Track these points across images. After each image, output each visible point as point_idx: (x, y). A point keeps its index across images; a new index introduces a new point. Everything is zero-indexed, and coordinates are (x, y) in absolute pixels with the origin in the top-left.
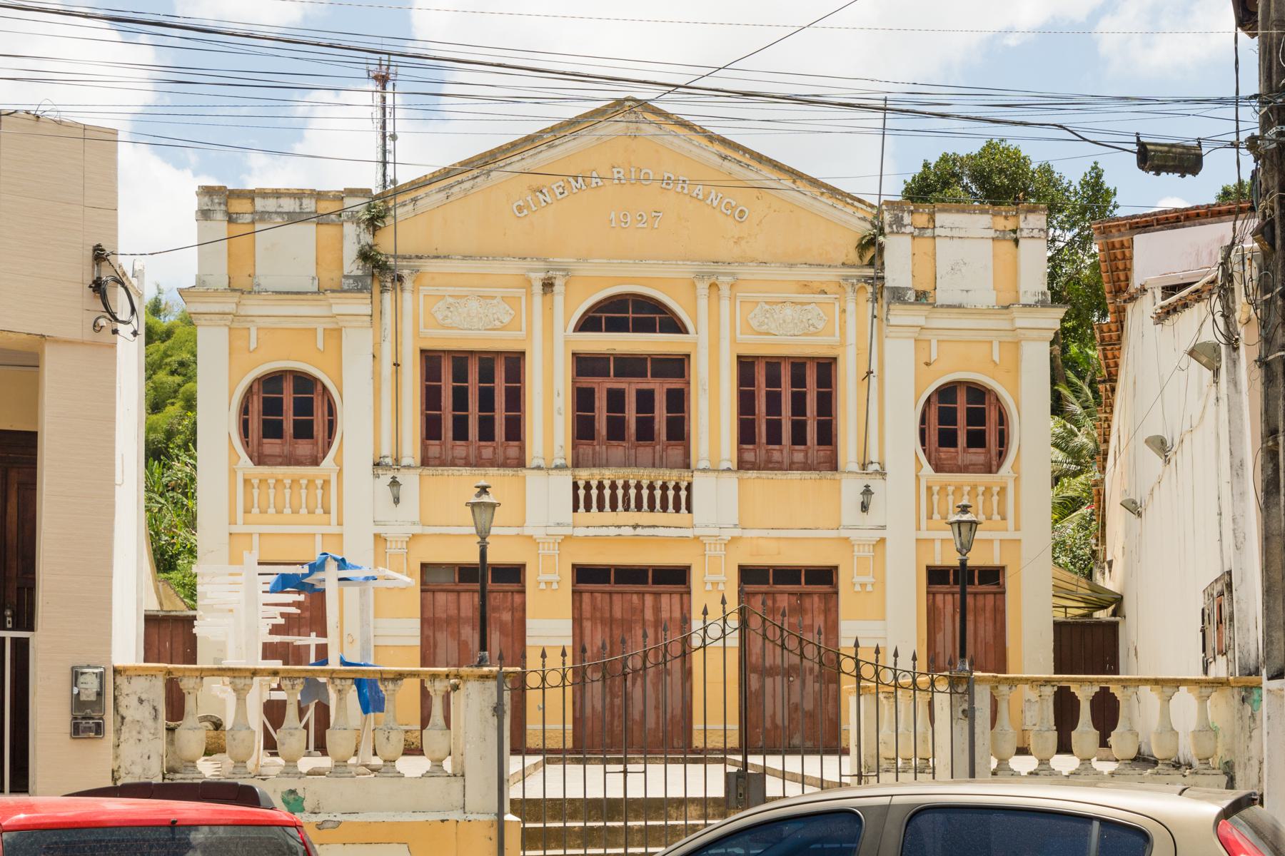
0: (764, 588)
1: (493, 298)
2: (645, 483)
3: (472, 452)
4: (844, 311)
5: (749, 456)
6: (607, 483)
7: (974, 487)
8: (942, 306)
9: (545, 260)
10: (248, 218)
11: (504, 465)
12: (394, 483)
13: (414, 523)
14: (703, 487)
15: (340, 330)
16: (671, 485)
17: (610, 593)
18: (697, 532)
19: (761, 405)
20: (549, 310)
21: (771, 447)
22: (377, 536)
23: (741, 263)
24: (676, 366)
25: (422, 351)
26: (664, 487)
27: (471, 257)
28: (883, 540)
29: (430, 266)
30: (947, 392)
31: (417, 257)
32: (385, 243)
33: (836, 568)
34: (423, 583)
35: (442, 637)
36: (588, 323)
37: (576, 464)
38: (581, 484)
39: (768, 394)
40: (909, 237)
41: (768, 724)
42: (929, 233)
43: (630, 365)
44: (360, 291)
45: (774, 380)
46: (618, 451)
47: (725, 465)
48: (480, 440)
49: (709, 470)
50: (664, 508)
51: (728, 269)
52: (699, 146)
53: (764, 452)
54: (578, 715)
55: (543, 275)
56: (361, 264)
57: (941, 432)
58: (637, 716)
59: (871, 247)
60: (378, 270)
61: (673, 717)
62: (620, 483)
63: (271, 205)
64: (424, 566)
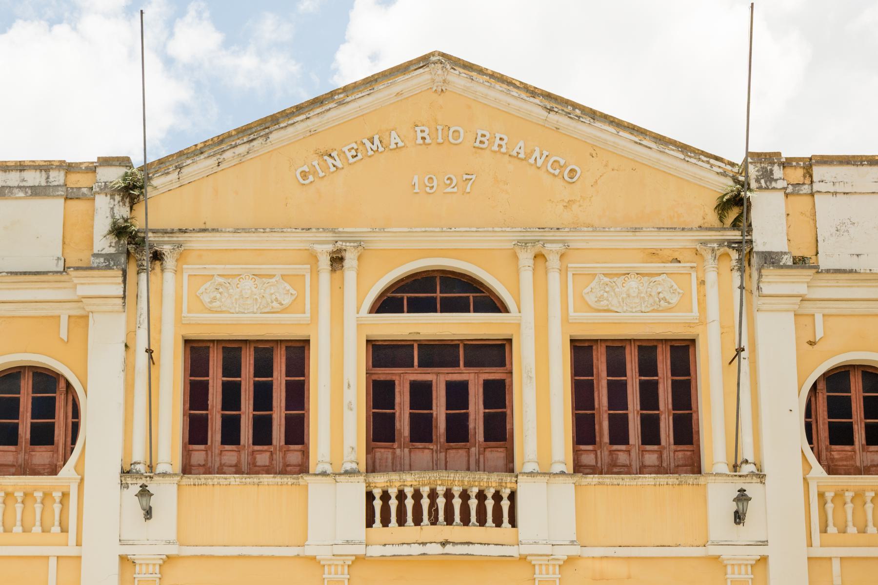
1: (272, 276)
2: (457, 490)
3: (245, 457)
4: (703, 282)
5: (588, 459)
6: (409, 491)
9: (333, 231)
11: (283, 472)
12: (144, 492)
14: (531, 496)
15: (86, 317)
16: (490, 493)
18: (524, 550)
19: (602, 397)
20: (338, 290)
21: (615, 447)
22: (123, 559)
23: (575, 229)
24: (496, 352)
25: (187, 342)
26: (481, 496)
27: (246, 230)
28: (764, 559)
29: (197, 242)
36: (387, 303)
37: (372, 468)
38: (377, 493)
39: (610, 384)
40: (781, 194)
42: (806, 189)
43: (438, 353)
45: (616, 367)
46: (423, 454)
47: (557, 468)
48: (254, 444)
49: (538, 474)
51: (558, 236)
53: (606, 453)
55: (330, 247)
56: (113, 239)
57: (832, 427)
59: (735, 205)
60: (135, 247)
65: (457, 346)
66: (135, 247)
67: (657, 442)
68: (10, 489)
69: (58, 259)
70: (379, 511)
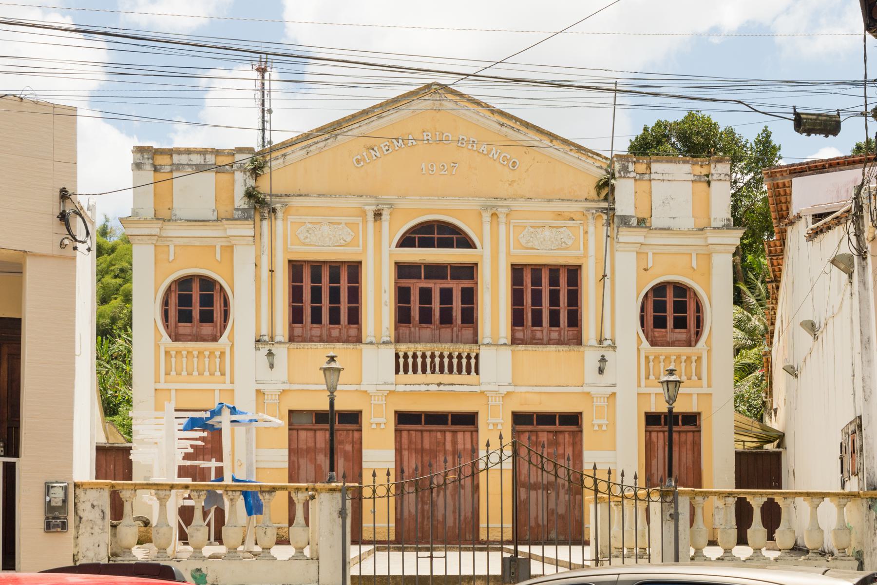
0: (529, 428)
1: (339, 224)
2: (446, 354)
4: (587, 232)
5: (519, 335)
6: (419, 354)
7: (679, 357)
8: (656, 229)
9: (376, 197)
10: (168, 168)
11: (347, 341)
13: (284, 382)
14: (487, 356)
16: (464, 355)
17: (422, 431)
18: (483, 388)
19: (528, 299)
20: (378, 233)
21: (535, 328)
22: (258, 391)
23: (514, 199)
24: (468, 271)
25: (290, 261)
26: (460, 357)
28: (614, 394)
29: (295, 202)
30: (659, 289)
31: (286, 195)
32: (264, 186)
33: (581, 413)
34: (290, 424)
35: (303, 462)
36: (406, 242)
37: (398, 340)
38: (401, 354)
41: (533, 523)
42: (647, 177)
43: (436, 271)
44: (246, 219)
45: (536, 281)
47: (502, 341)
48: (330, 323)
50: (460, 371)
51: (505, 203)
52: (484, 117)
54: (399, 517)
55: (374, 208)
56: (247, 200)
57: (655, 317)
58: (440, 518)
59: (605, 187)
60: (259, 204)
61: (465, 518)
62: (428, 354)
63: (183, 159)
64: (291, 412)
65: (446, 267)
66: (259, 204)
67: (558, 326)
68: (190, 350)
69: (214, 211)
70: (402, 365)
